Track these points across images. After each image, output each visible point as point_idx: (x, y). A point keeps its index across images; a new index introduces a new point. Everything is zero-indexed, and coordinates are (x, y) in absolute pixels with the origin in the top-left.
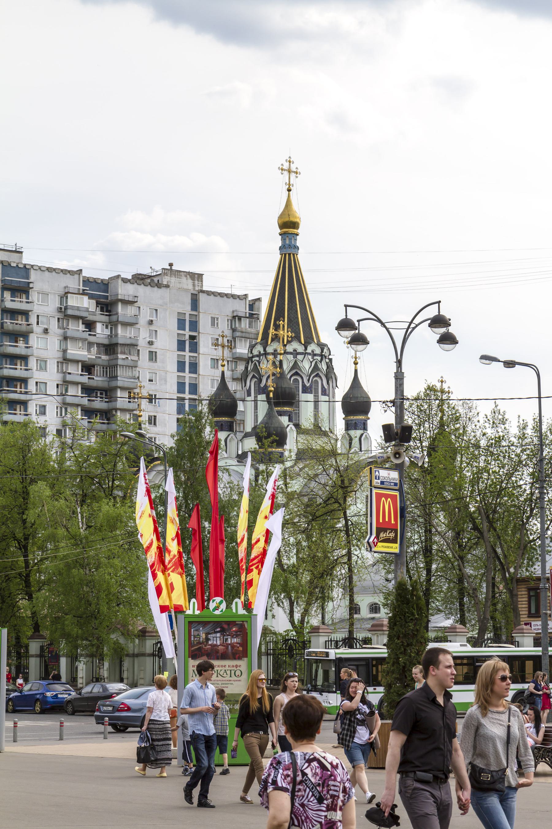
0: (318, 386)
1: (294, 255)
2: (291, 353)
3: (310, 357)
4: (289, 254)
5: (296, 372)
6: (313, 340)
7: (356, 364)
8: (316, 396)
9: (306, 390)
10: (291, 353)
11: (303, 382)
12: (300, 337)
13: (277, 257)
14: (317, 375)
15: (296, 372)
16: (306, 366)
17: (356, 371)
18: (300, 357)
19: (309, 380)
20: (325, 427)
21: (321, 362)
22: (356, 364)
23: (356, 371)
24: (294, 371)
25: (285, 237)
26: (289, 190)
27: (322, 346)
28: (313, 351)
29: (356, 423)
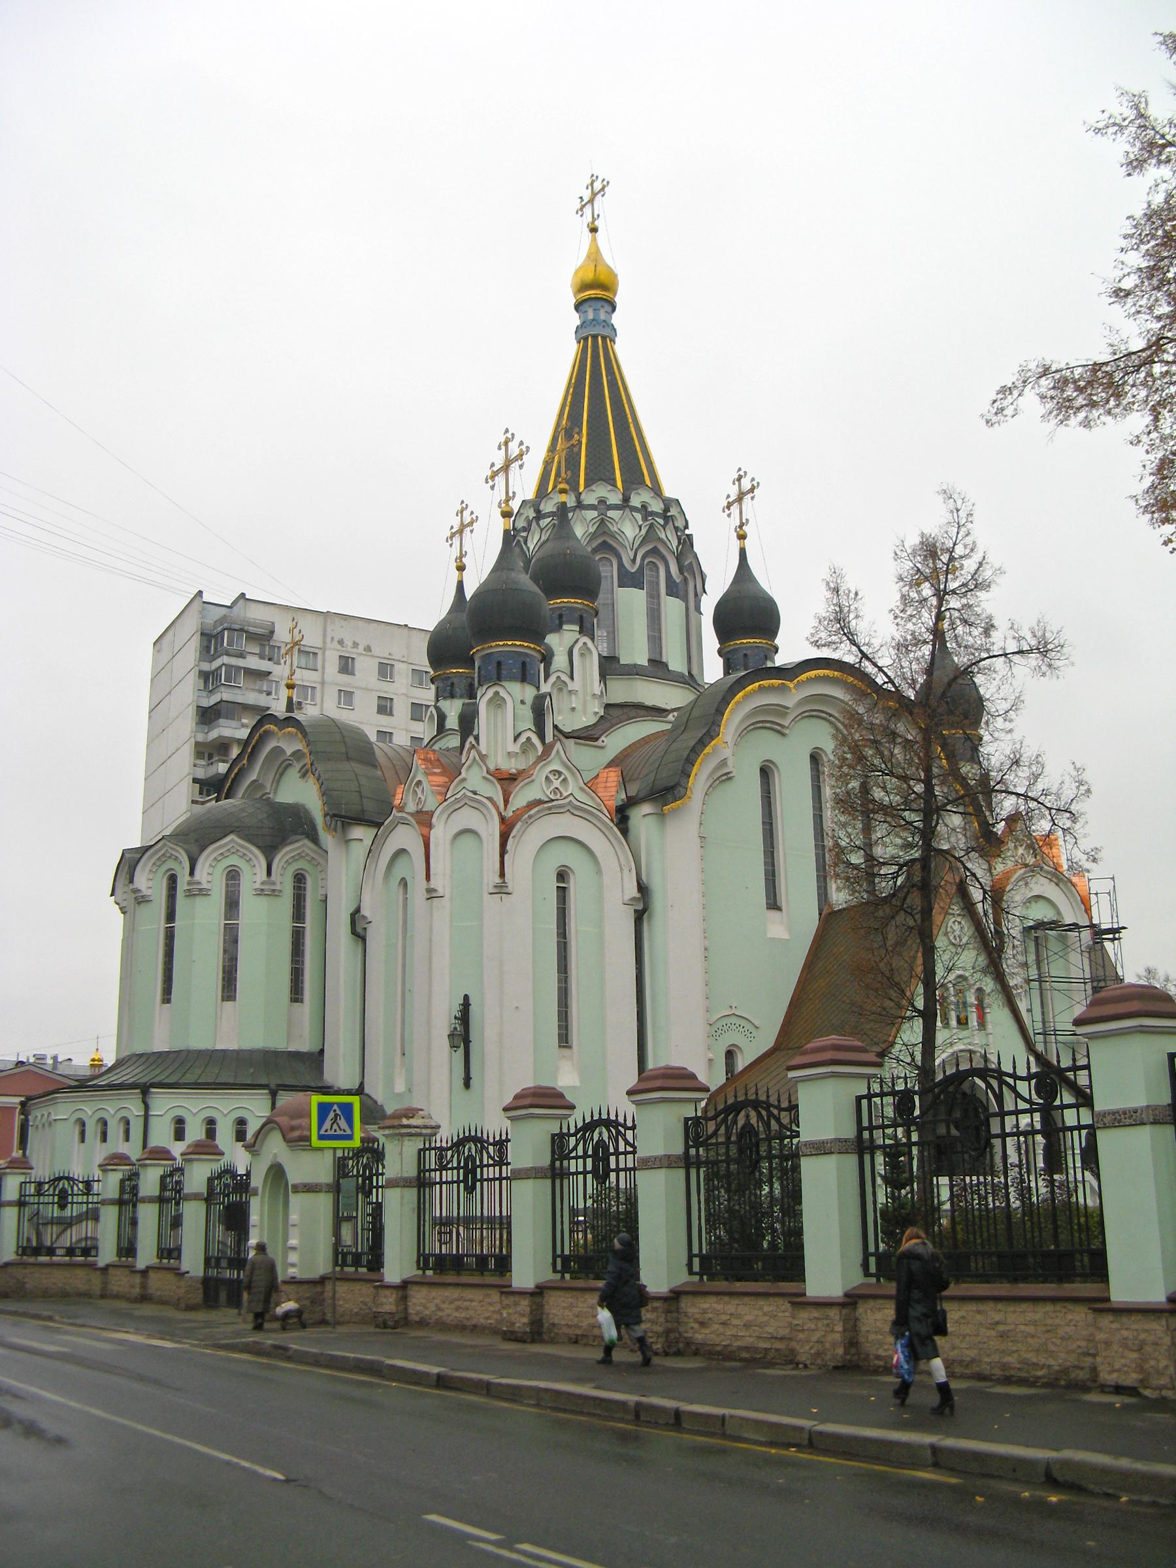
0: (658, 577)
1: (604, 338)
2: (592, 507)
3: (638, 516)
4: (595, 337)
5: (605, 542)
6: (643, 483)
7: (742, 537)
8: (654, 597)
9: (630, 580)
10: (592, 507)
11: (621, 565)
12: (614, 480)
13: (569, 350)
14: (655, 551)
15: (605, 542)
16: (629, 529)
17: (743, 553)
18: (610, 513)
19: (634, 561)
20: (676, 663)
21: (664, 527)
22: (742, 537)
23: (743, 553)
24: (600, 541)
25: (585, 307)
26: (594, 230)
27: (670, 503)
28: (644, 507)
29: (745, 655)
